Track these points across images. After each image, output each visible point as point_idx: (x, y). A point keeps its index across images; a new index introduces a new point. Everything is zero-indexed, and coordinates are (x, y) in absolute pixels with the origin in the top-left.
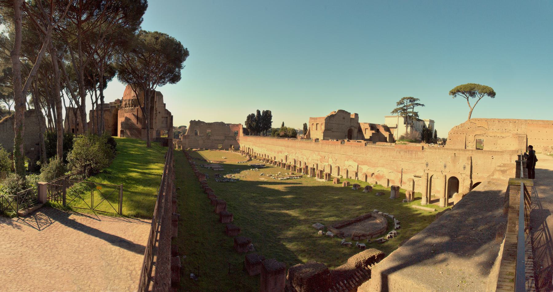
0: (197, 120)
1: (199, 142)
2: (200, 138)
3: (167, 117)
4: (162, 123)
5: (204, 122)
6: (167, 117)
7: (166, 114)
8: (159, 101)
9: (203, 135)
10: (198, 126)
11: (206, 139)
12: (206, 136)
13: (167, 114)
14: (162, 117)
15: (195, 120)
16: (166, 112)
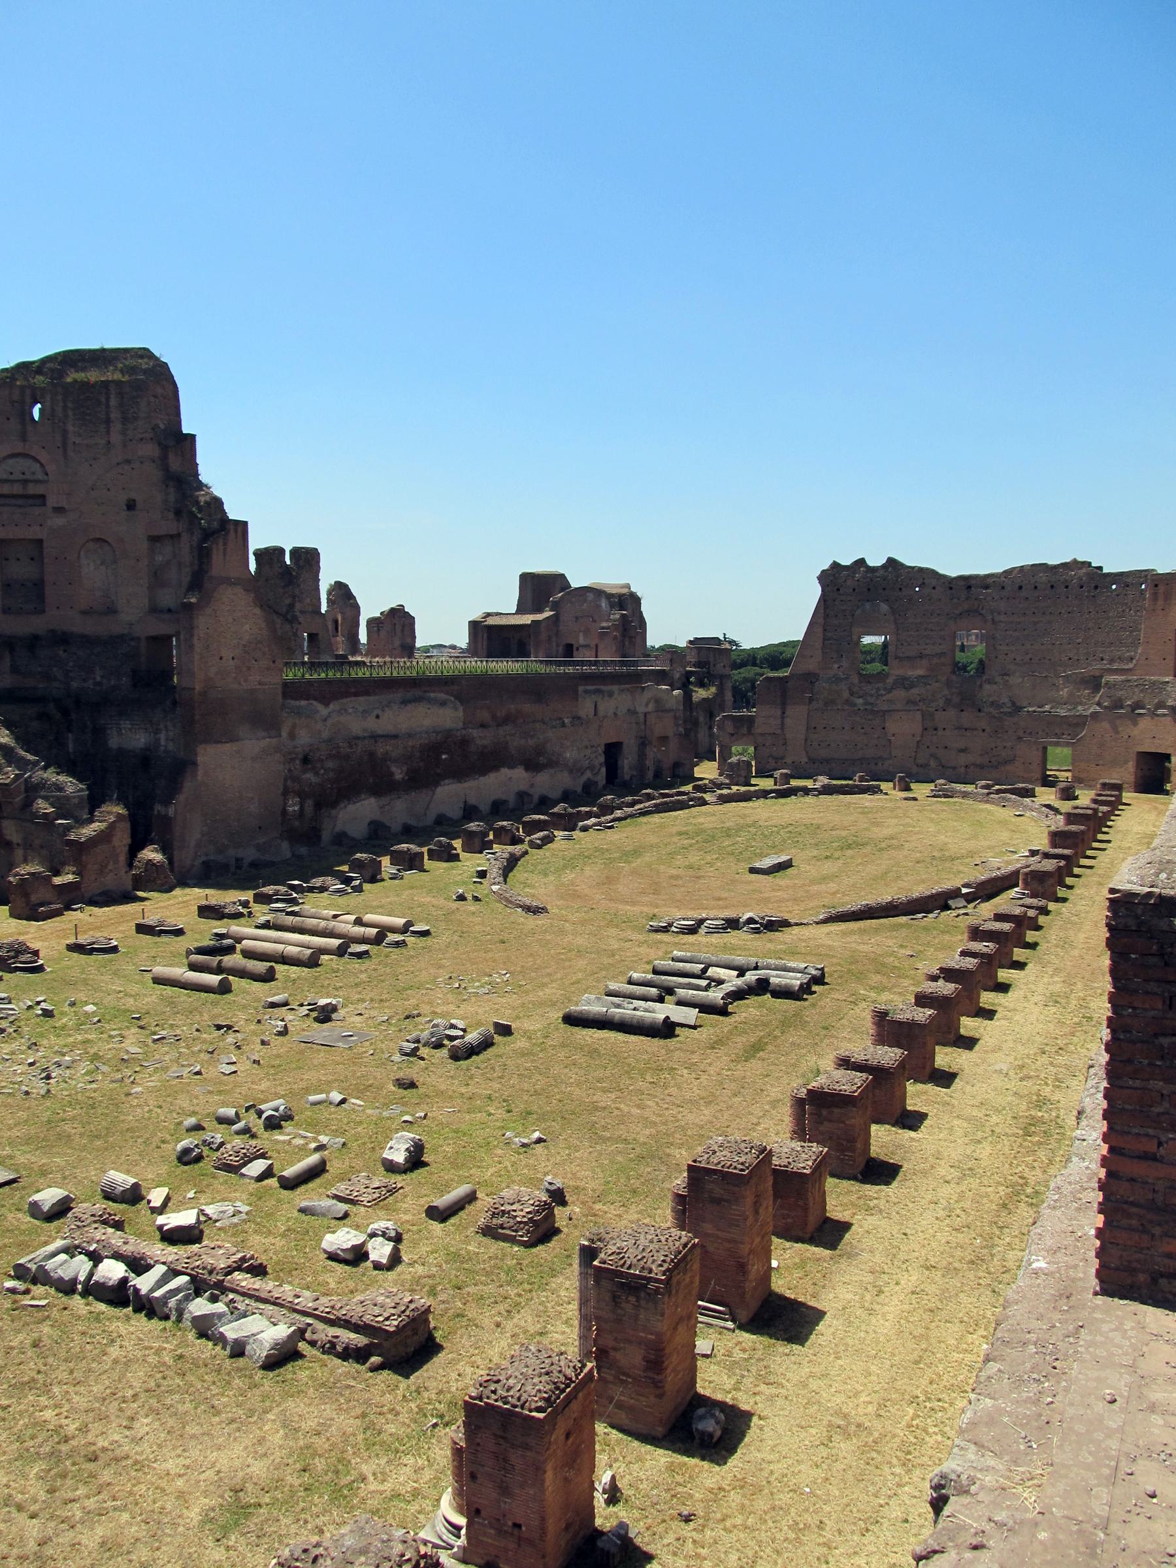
0: (876, 560)
1: (892, 726)
2: (900, 693)
3: (179, 535)
4: (157, 578)
5: (933, 573)
6: (179, 535)
7: (171, 515)
8: (125, 420)
9: (920, 672)
10: (884, 607)
11: (948, 701)
12: (949, 684)
13: (178, 513)
14: (154, 539)
15: (861, 562)
16: (172, 498)
